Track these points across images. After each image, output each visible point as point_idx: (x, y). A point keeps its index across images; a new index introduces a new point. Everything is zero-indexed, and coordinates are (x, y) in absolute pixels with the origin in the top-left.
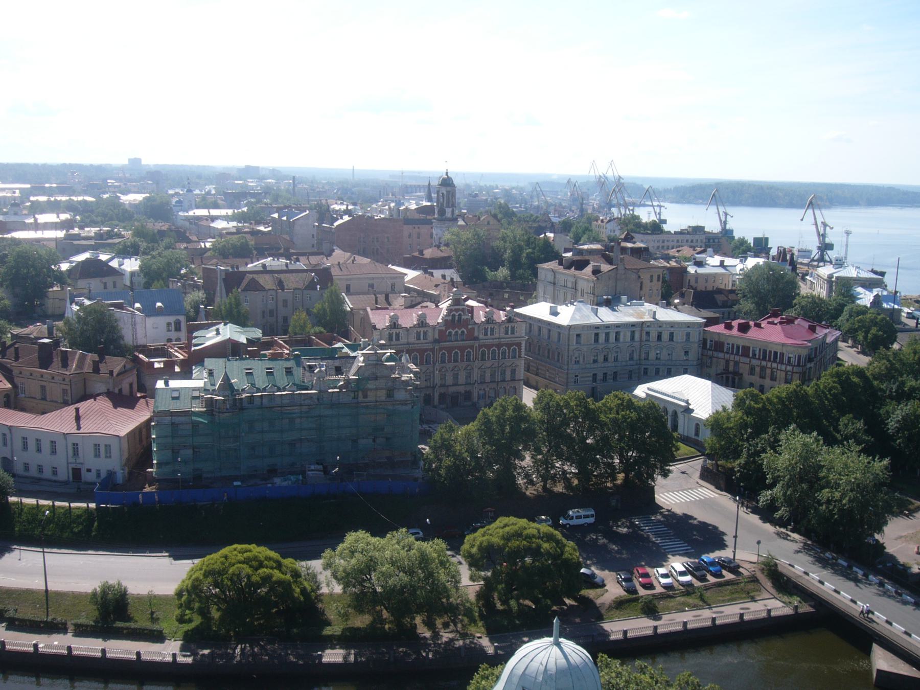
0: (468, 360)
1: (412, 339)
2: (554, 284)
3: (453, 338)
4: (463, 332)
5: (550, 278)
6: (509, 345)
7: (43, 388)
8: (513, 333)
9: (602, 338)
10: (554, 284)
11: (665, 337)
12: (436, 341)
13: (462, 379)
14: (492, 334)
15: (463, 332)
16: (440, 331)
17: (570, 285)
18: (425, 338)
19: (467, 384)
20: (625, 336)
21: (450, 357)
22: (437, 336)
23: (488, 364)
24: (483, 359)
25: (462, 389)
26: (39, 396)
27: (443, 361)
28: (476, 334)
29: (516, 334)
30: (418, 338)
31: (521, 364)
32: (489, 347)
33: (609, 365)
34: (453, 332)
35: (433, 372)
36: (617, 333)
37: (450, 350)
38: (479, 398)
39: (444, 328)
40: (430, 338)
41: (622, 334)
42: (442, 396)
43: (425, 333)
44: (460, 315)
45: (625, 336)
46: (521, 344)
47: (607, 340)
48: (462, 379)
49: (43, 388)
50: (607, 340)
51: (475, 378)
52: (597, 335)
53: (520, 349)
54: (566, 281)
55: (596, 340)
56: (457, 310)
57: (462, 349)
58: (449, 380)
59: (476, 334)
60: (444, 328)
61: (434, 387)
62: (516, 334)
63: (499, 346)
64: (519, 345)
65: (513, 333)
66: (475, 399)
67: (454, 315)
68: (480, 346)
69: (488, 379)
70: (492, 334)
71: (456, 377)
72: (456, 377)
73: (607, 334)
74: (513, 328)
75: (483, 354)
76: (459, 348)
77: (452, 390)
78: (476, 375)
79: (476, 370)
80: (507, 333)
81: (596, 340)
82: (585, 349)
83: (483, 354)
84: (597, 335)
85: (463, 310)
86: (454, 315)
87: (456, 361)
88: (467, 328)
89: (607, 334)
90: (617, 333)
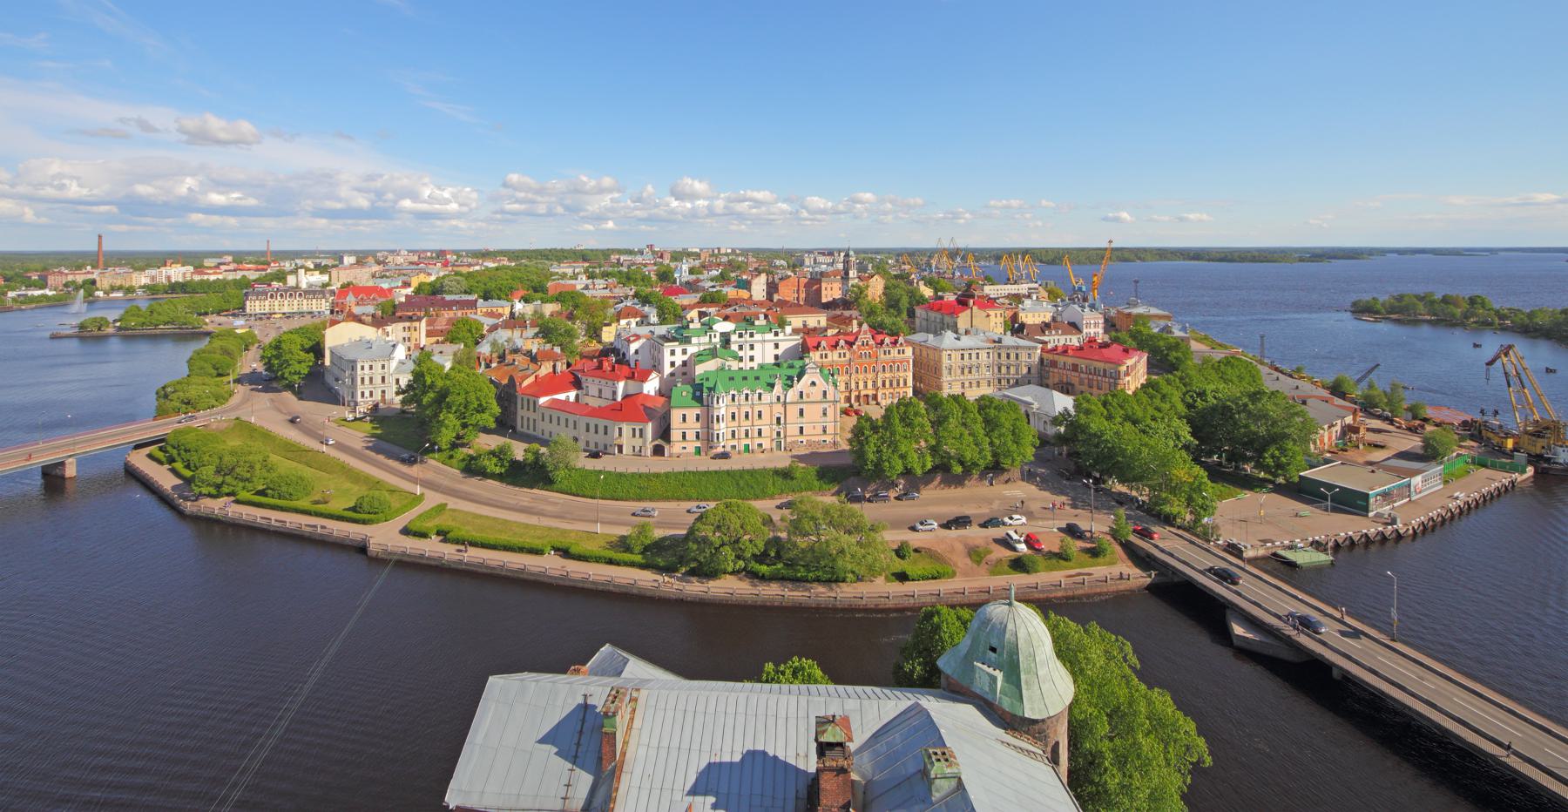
1: (836, 357)
11: (1013, 356)
13: (870, 384)
20: (983, 355)
25: (870, 393)
42: (858, 398)
48: (870, 384)
78: (880, 384)
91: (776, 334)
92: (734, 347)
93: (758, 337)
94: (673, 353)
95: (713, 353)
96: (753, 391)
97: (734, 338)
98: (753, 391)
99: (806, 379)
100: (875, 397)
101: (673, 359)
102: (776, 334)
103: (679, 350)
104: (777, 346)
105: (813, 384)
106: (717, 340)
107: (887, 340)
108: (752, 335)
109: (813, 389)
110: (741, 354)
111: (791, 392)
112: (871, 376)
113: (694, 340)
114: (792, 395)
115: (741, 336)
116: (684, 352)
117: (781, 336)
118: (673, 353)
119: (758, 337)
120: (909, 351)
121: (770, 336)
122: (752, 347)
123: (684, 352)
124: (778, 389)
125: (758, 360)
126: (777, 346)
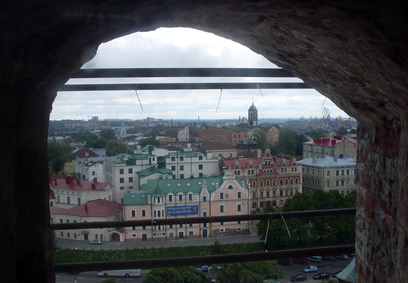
0: (274, 184)
1: (246, 174)
2: (312, 152)
3: (266, 173)
4: (271, 170)
5: (310, 149)
6: (294, 177)
7: (69, 198)
8: (296, 171)
9: (340, 173)
10: (312, 152)
12: (257, 175)
13: (271, 194)
14: (286, 171)
15: (271, 170)
16: (260, 170)
17: (320, 151)
18: (252, 173)
19: (274, 197)
21: (265, 183)
22: (258, 173)
23: (284, 187)
24: (281, 184)
25: (271, 200)
26: (67, 202)
27: (262, 185)
28: (278, 172)
29: (298, 171)
30: (249, 173)
31: (301, 187)
32: (284, 178)
33: (345, 187)
34: (266, 171)
35: (257, 191)
36: (348, 171)
37: (265, 179)
38: (280, 204)
39: (262, 168)
40: (255, 173)
41: (350, 171)
43: (252, 171)
44: (269, 162)
45: (351, 172)
46: (300, 176)
47: (343, 174)
48: (271, 194)
49: (69, 198)
50: (343, 174)
51: (278, 194)
52: (337, 171)
53: (300, 179)
54: (318, 149)
55: (337, 174)
56: (268, 159)
57: (271, 179)
58: (265, 195)
59: (278, 172)
60: (262, 168)
61: (257, 199)
62: (298, 171)
63: (289, 177)
64: (299, 177)
65: (296, 171)
66: (278, 205)
67: (266, 162)
68: (280, 178)
69: (284, 194)
70: (286, 171)
71: (268, 193)
72: (268, 193)
73: (343, 171)
74: (296, 168)
75: (281, 181)
76: (269, 178)
77: (266, 200)
78: (278, 193)
79: (278, 190)
80: (293, 171)
81: (337, 174)
82: (332, 179)
83: (281, 181)
84: (337, 171)
85: (271, 159)
86: (266, 162)
87: (268, 185)
88: (273, 168)
89: (343, 171)
90: (348, 171)
91: (201, 158)
92: (169, 167)
93: (186, 160)
94: (122, 172)
95: (152, 170)
96: (185, 194)
97: (168, 161)
98: (185, 194)
99: (226, 184)
100: (274, 203)
101: (122, 176)
102: (201, 158)
103: (126, 169)
104: (201, 167)
105: (230, 187)
106: (155, 162)
107: (284, 161)
108: (182, 159)
109: (230, 192)
110: (174, 173)
111: (213, 195)
112: (271, 188)
113: (138, 162)
114: (214, 196)
115: (173, 159)
116: (131, 171)
117: (204, 159)
118: (122, 172)
119: (186, 160)
120: (300, 169)
121: (197, 159)
122: (182, 168)
123: (131, 171)
124: (205, 192)
125: (187, 175)
126: (201, 167)
